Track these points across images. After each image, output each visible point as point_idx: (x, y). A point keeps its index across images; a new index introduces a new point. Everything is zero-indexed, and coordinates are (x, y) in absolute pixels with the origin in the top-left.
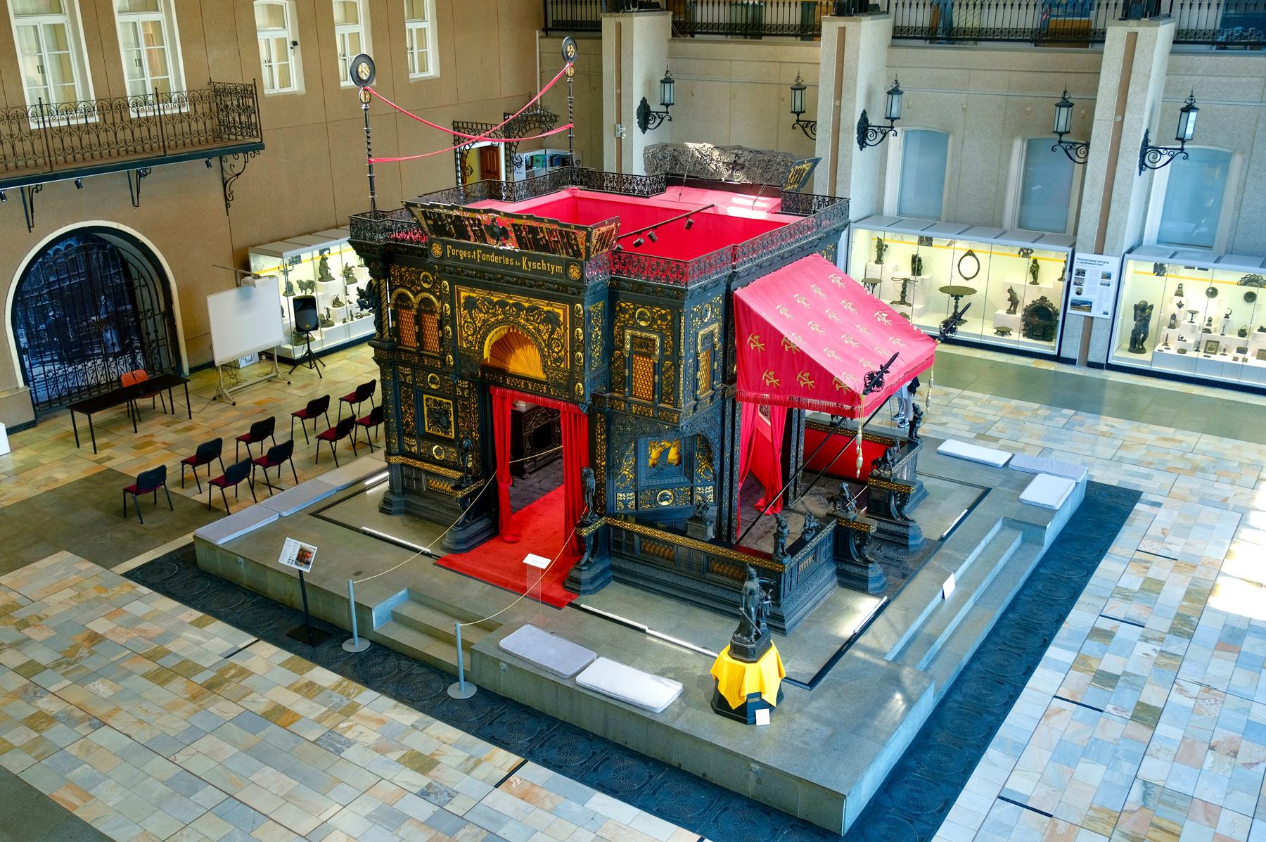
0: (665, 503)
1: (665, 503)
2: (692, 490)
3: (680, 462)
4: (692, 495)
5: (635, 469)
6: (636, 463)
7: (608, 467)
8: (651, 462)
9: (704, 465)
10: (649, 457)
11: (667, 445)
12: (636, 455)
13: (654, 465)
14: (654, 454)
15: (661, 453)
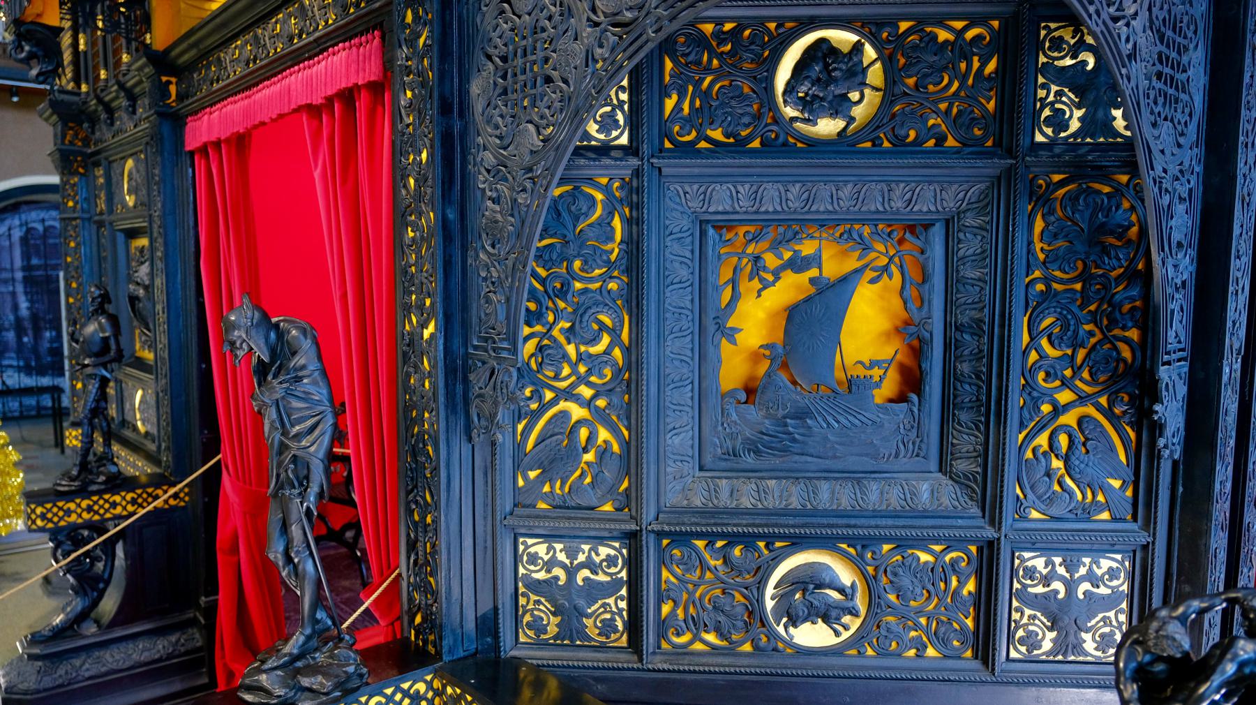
0: (813, 635)
1: (813, 635)
2: (988, 564)
3: (912, 382)
4: (986, 603)
5: (629, 388)
6: (633, 351)
7: (457, 370)
8: (733, 367)
9: (1072, 404)
10: (712, 325)
11: (832, 267)
12: (634, 300)
13: (750, 391)
14: (756, 317)
15: (794, 315)
